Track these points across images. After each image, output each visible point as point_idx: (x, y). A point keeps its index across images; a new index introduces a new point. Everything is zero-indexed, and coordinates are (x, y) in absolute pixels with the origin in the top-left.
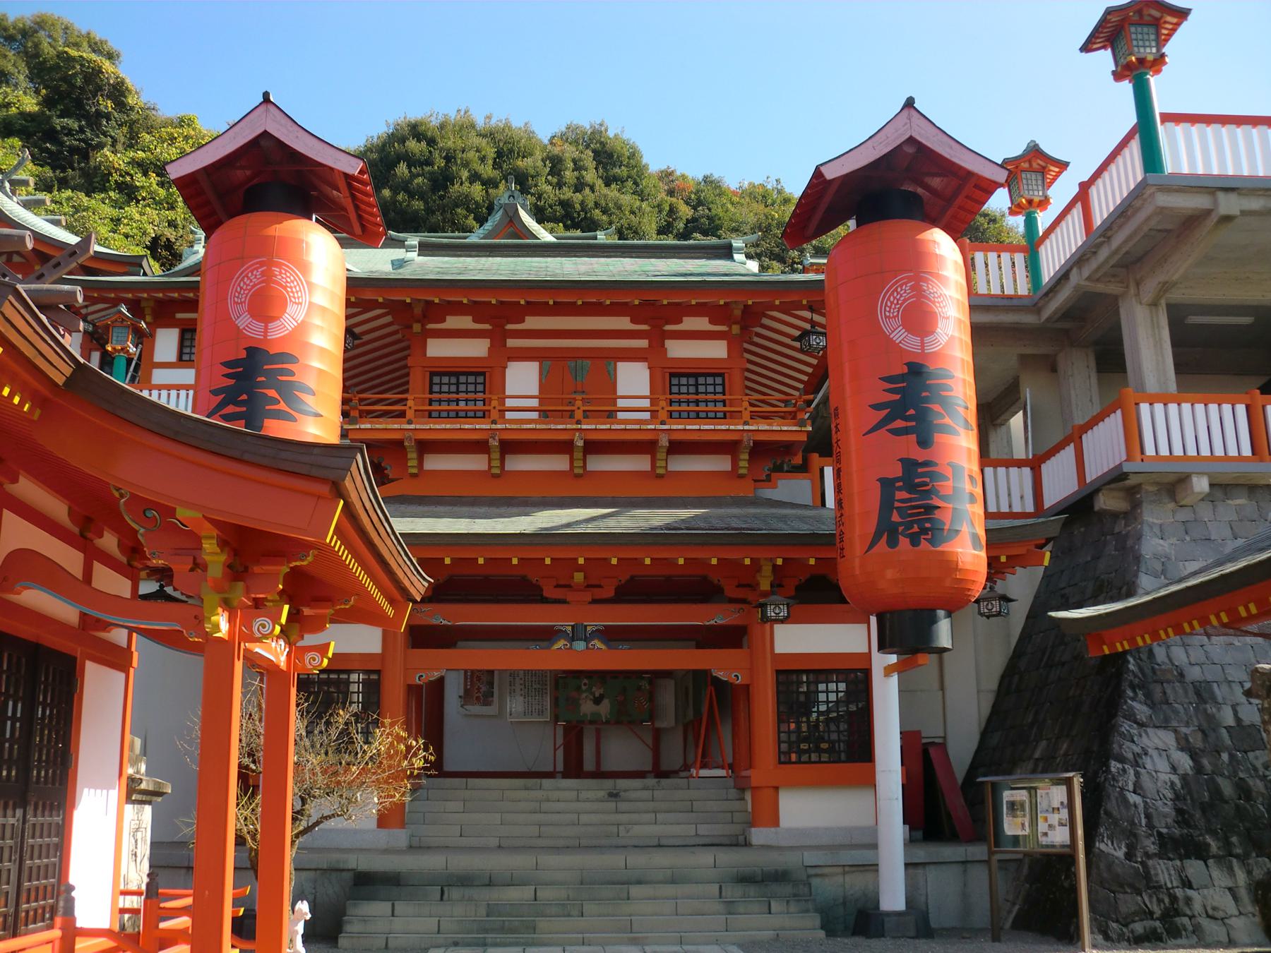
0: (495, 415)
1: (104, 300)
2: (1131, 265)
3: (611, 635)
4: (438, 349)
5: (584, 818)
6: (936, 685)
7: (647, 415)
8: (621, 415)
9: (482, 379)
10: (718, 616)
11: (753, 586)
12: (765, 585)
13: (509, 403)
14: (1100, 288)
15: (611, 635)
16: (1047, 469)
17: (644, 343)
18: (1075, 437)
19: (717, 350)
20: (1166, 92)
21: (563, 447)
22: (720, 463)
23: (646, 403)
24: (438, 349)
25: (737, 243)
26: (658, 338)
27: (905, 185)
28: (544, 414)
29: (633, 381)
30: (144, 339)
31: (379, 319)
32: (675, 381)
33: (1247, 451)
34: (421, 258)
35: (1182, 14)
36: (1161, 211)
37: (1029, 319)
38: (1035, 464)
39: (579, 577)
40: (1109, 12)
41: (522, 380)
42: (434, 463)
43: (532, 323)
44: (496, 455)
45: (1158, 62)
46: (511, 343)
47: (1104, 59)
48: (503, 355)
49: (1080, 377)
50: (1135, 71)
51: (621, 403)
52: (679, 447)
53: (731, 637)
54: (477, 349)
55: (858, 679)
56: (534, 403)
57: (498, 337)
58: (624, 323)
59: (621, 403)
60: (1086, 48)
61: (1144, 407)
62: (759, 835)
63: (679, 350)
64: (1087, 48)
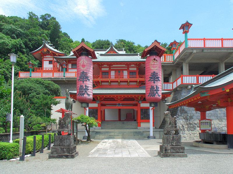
0: (110, 78)
1: (61, 60)
2: (184, 59)
3: (122, 104)
4: (103, 69)
5: (120, 126)
6: (159, 111)
7: (127, 78)
8: (124, 78)
9: (108, 73)
10: (134, 102)
11: (138, 99)
12: (139, 99)
13: (111, 76)
14: (180, 61)
15: (122, 104)
16: (174, 84)
17: (127, 68)
18: (176, 80)
19: (135, 69)
20: (189, 35)
21: (118, 82)
22: (135, 83)
23: (127, 76)
24: (103, 69)
25: (138, 54)
26: (128, 67)
27: (155, 51)
28: (115, 78)
29: (125, 73)
30: (67, 65)
31: (96, 65)
32: (130, 73)
33: (196, 83)
34: (101, 56)
35: (191, 25)
36: (186, 52)
37: (172, 65)
38: (173, 83)
39: (119, 98)
40: (182, 25)
41: (113, 73)
42: (103, 84)
43: (114, 66)
44: (110, 83)
45: (188, 32)
46: (111, 68)
47: (182, 30)
48: (110, 70)
49: (178, 72)
50: (186, 32)
51: (124, 76)
52: (130, 82)
53: (136, 105)
54: (107, 69)
55: (148, 109)
56: (114, 76)
57: (110, 68)
58: (124, 66)
59: (124, 76)
60: (180, 29)
61: (184, 77)
62: (138, 128)
63: (131, 69)
64: (180, 29)
